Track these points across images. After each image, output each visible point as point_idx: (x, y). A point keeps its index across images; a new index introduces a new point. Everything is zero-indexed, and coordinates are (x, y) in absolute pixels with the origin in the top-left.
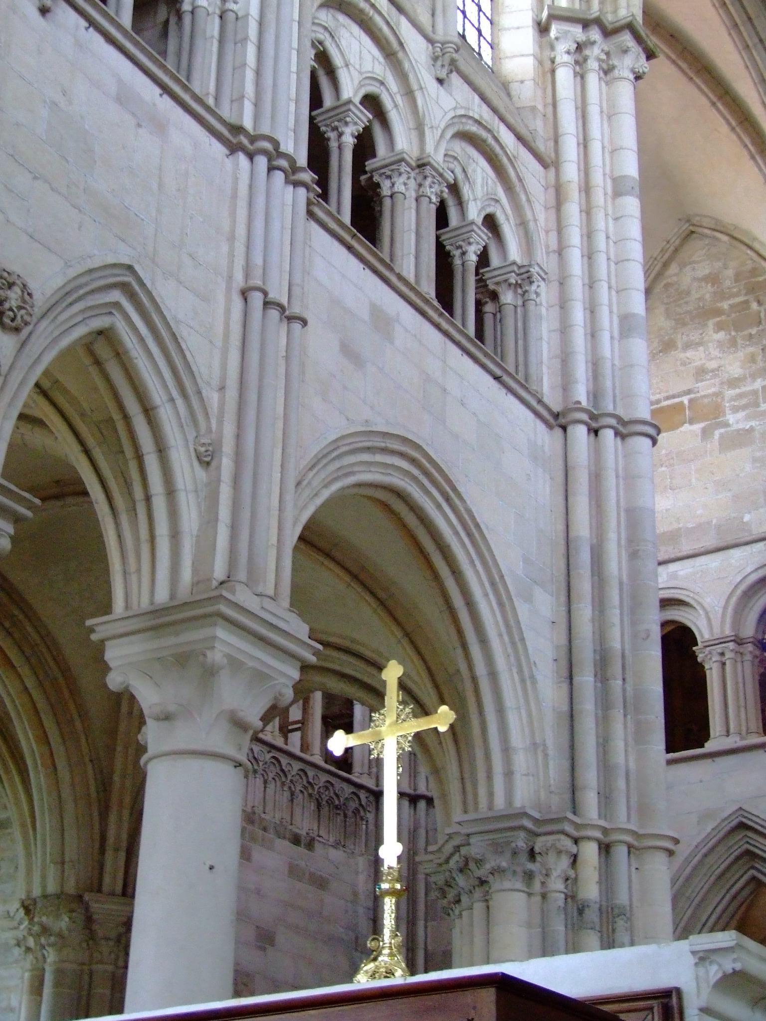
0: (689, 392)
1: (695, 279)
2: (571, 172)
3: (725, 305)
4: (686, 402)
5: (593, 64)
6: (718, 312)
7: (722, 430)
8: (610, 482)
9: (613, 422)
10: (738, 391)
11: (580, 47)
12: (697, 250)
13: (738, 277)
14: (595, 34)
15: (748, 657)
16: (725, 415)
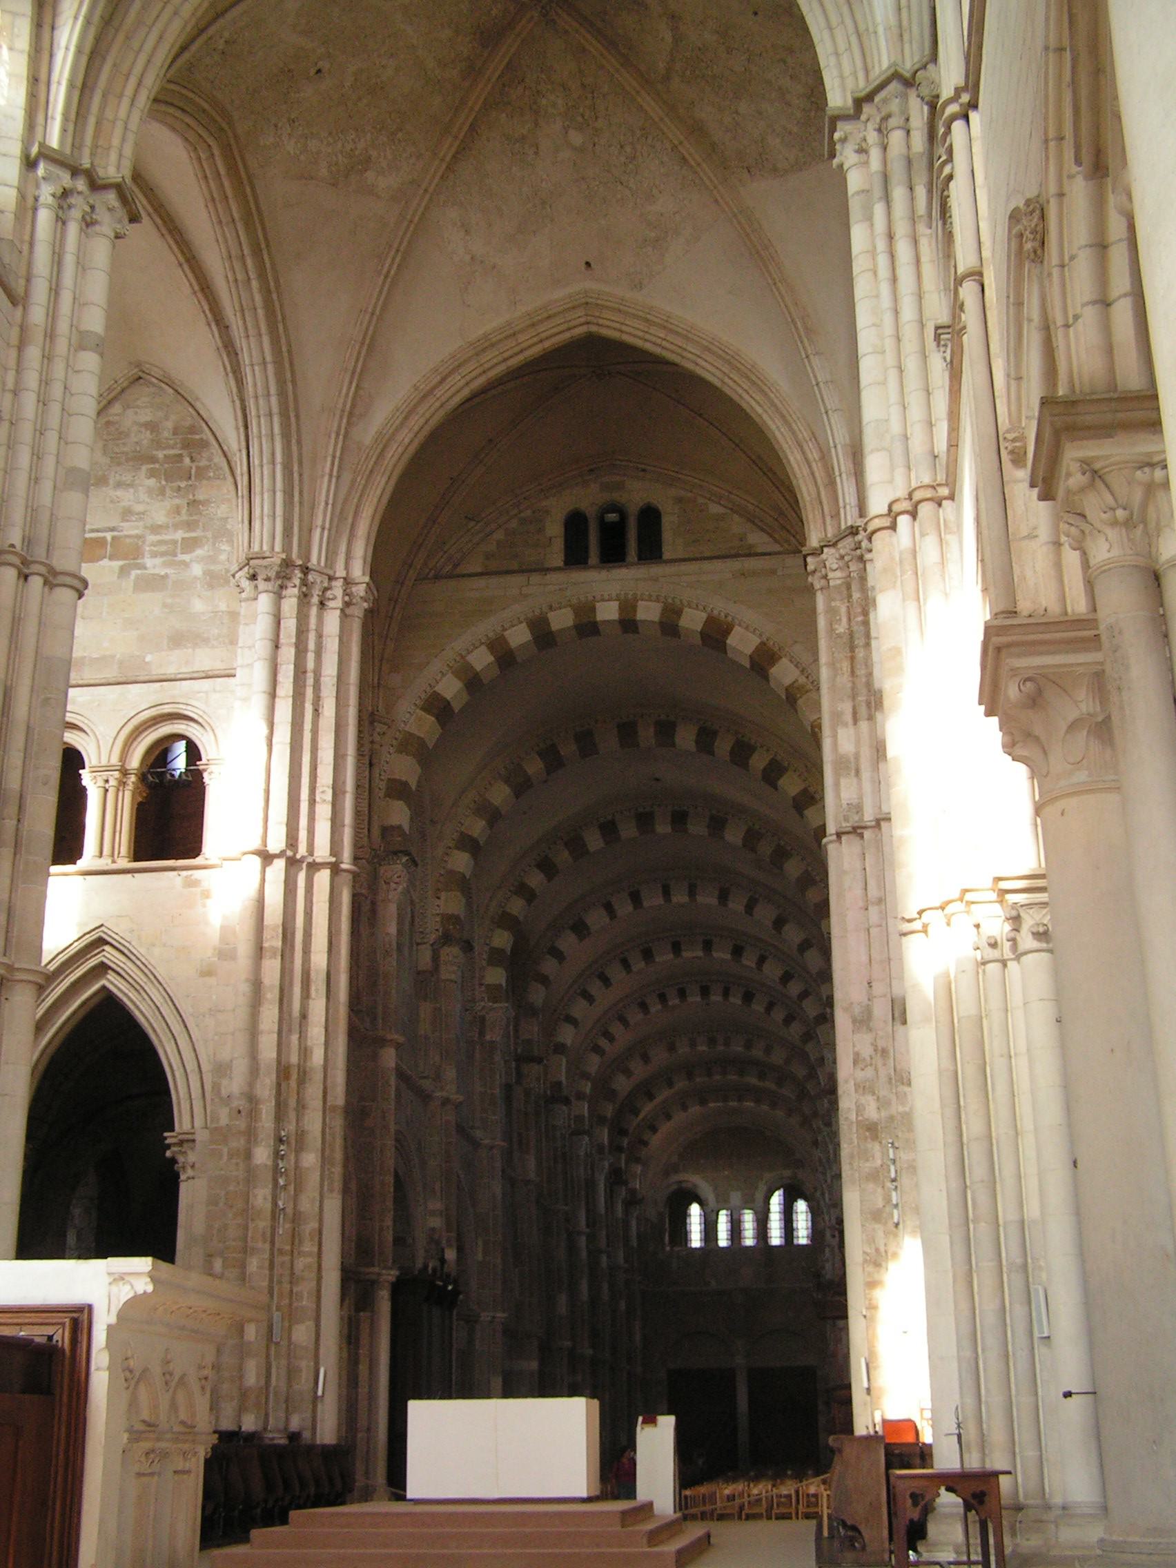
0: (112, 529)
1: (135, 423)
2: (37, 315)
3: (160, 455)
4: (109, 539)
5: (76, 214)
6: (153, 460)
7: (139, 572)
8: (30, 628)
9: (43, 570)
10: (158, 538)
11: (66, 193)
12: (142, 396)
13: (175, 432)
14: (81, 184)
15: (130, 787)
16: (143, 558)
